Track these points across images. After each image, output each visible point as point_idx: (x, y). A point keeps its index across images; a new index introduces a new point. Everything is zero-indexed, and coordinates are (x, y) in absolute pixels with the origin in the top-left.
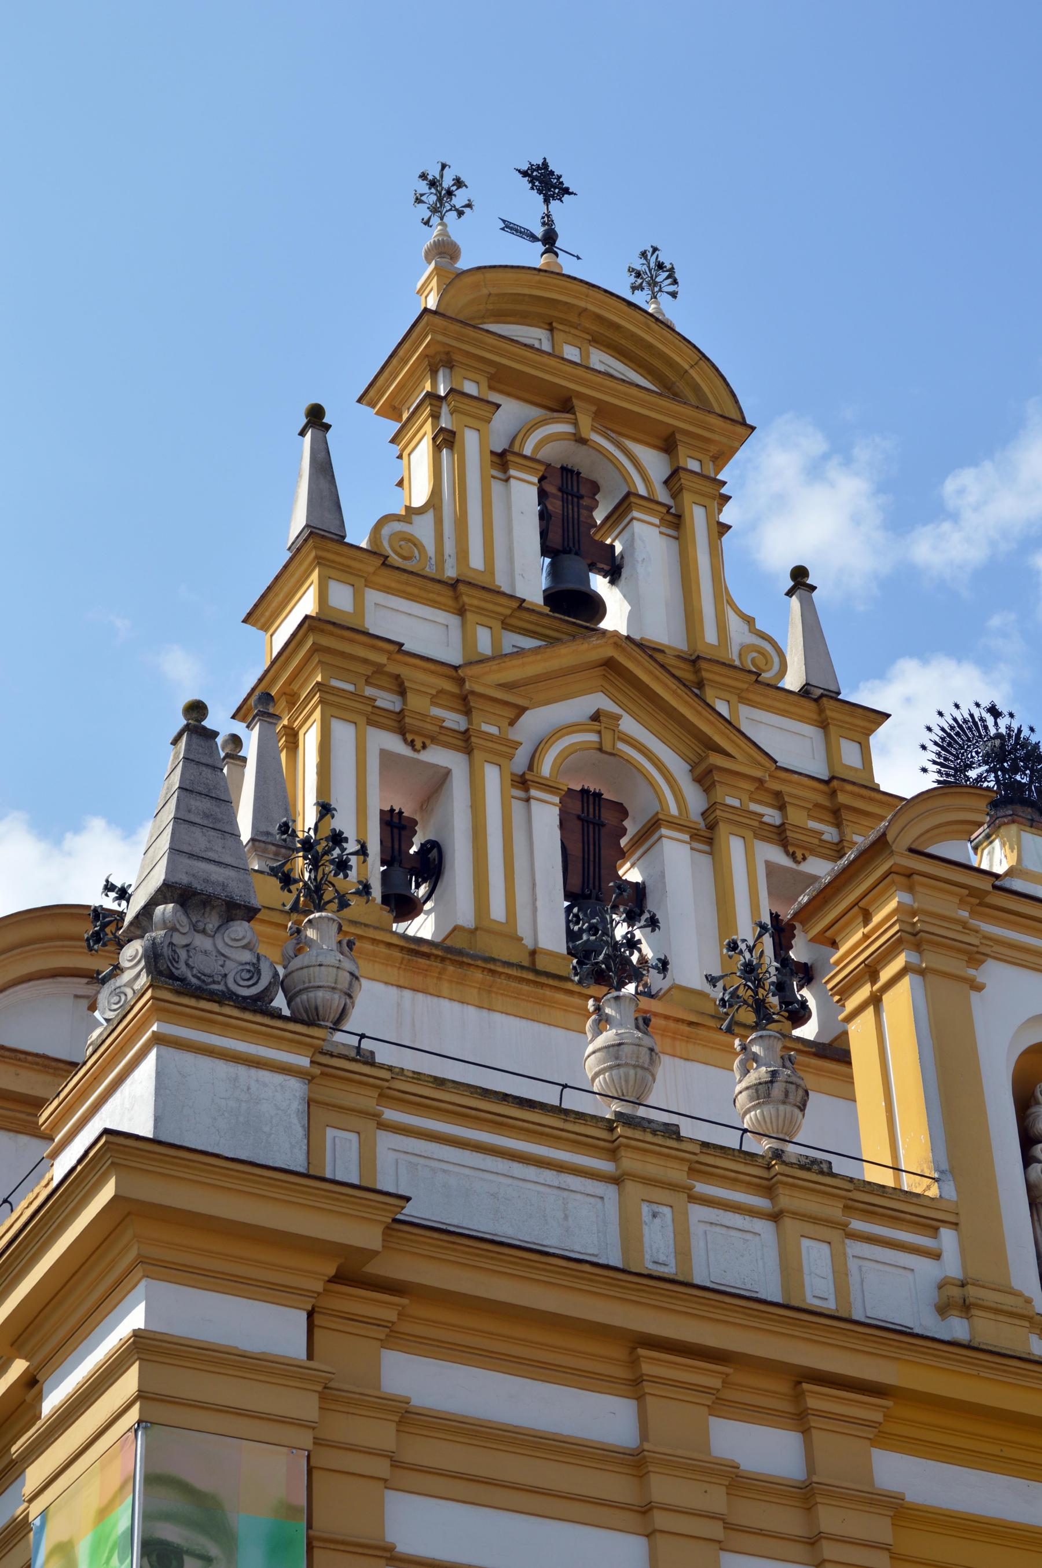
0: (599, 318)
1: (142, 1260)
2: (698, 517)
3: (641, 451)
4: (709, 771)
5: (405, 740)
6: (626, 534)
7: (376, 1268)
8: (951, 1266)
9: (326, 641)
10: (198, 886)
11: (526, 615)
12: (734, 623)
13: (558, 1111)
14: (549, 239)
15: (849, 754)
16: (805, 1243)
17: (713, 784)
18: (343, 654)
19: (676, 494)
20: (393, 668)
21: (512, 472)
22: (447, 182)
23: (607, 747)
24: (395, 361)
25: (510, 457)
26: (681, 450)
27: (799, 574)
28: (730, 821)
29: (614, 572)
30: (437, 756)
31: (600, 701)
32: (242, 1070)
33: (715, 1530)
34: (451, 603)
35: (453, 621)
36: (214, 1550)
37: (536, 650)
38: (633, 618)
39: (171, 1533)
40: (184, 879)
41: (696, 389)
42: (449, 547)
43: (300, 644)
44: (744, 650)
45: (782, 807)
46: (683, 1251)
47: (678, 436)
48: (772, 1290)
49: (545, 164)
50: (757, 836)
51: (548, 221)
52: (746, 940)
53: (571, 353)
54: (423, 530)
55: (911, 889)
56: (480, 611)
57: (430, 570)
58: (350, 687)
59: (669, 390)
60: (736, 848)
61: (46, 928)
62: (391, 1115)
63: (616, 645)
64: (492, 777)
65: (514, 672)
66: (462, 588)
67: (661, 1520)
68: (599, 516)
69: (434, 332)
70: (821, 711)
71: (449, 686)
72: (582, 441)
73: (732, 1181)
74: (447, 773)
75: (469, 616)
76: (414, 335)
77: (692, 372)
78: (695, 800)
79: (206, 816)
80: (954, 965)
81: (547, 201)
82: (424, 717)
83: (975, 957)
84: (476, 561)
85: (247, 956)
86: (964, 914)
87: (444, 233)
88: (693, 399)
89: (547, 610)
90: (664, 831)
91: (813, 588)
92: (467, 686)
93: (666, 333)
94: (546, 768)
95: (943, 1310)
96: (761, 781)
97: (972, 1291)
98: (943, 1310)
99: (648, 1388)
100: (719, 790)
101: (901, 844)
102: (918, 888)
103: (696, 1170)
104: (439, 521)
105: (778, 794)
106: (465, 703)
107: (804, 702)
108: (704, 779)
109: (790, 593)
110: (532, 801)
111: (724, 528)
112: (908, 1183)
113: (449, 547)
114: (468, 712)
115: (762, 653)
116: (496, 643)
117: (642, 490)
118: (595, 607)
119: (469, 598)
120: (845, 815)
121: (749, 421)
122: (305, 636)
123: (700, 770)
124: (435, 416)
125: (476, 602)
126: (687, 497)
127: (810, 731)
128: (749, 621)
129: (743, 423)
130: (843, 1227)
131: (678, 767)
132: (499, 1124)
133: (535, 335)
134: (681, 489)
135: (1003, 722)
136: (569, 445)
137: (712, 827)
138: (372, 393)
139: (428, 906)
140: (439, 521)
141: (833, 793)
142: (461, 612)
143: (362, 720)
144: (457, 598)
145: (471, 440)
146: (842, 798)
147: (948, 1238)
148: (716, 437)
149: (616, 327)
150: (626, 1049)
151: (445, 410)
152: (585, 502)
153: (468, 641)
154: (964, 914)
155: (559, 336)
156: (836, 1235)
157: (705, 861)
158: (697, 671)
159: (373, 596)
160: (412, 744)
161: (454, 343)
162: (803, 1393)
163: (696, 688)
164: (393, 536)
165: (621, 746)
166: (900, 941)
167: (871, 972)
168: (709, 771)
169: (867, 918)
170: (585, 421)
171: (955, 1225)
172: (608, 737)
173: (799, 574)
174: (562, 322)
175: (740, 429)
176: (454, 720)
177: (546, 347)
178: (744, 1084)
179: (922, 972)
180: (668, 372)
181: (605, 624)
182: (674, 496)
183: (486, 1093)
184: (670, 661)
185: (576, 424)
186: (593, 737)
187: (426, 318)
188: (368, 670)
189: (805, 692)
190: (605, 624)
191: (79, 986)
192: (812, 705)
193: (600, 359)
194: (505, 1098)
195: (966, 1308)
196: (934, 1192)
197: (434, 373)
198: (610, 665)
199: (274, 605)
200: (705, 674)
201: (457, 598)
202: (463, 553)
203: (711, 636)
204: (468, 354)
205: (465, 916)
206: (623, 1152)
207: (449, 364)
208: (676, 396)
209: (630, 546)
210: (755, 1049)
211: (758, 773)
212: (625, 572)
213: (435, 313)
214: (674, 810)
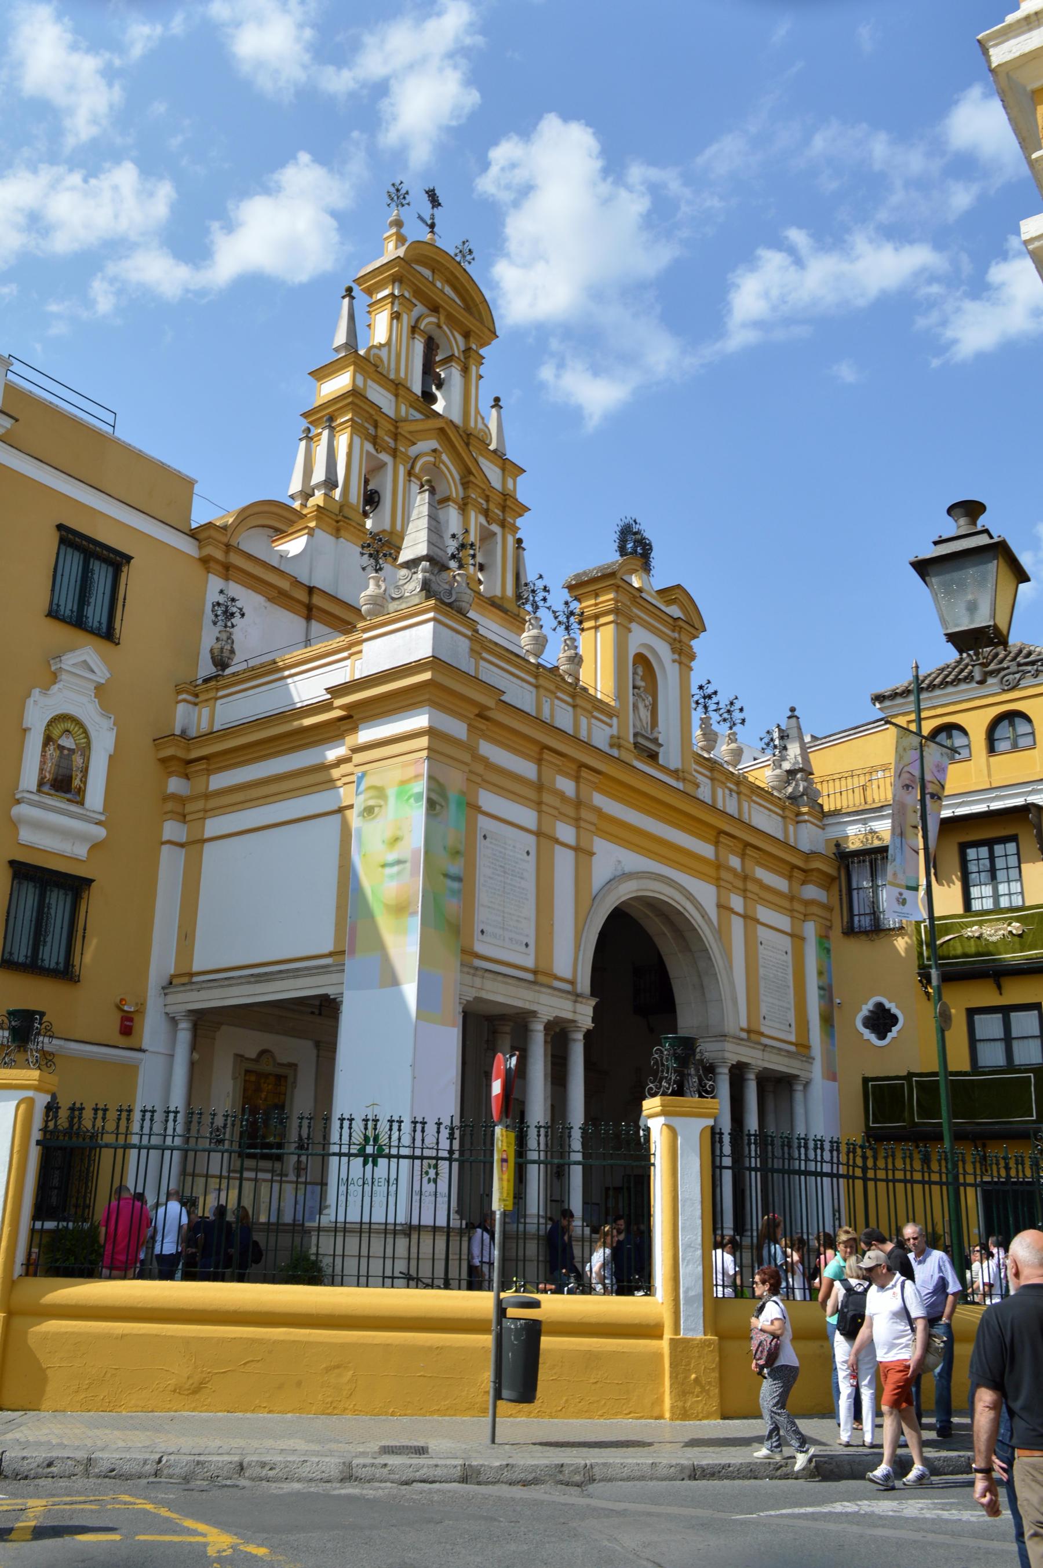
0: (452, 273)
1: (429, 700)
2: (473, 369)
3: (456, 334)
4: (468, 482)
5: (375, 447)
6: (447, 371)
7: (490, 714)
8: (614, 731)
9: (357, 401)
10: (435, 557)
11: (418, 402)
12: (480, 420)
13: (524, 659)
14: (432, 226)
16: (582, 717)
17: (468, 488)
18: (360, 407)
19: (467, 358)
20: (376, 417)
21: (416, 336)
22: (403, 191)
23: (437, 464)
24: (377, 271)
25: (417, 330)
26: (471, 339)
27: (497, 400)
28: (473, 505)
29: (439, 387)
30: (385, 457)
32: (454, 634)
33: (555, 813)
34: (394, 391)
35: (392, 398)
36: (443, 804)
37: (422, 420)
38: (445, 408)
39: (434, 797)
40: (431, 554)
41: (480, 313)
42: (393, 365)
43: (345, 398)
45: (487, 502)
46: (552, 716)
47: (472, 333)
48: (571, 731)
49: (433, 190)
50: (480, 513)
51: (433, 217)
52: (548, 591)
53: (439, 284)
54: (384, 353)
55: (617, 592)
56: (404, 397)
57: (385, 373)
58: (360, 421)
59: (468, 308)
60: (473, 514)
61: (266, 508)
62: (485, 655)
63: (446, 423)
64: (402, 471)
65: (413, 427)
66: (400, 386)
67: (544, 808)
68: (438, 359)
69: (399, 266)
70: (504, 464)
71: (392, 428)
72: (439, 327)
73: (564, 692)
74: (383, 465)
75: (400, 399)
76: (390, 265)
77: (480, 306)
79: (436, 528)
80: (625, 622)
81: (433, 208)
82: (384, 440)
83: (631, 620)
84: (402, 374)
85: (447, 587)
86: (629, 603)
87: (398, 215)
88: (477, 317)
89: (422, 400)
90: (450, 503)
91: (501, 408)
92: (399, 430)
93: (474, 286)
94: (417, 469)
95: (611, 746)
96: (484, 490)
97: (622, 741)
98: (611, 746)
99: (544, 763)
100: (470, 490)
101: (619, 576)
102: (620, 593)
103: (558, 687)
104: (389, 351)
105: (488, 496)
106: (396, 436)
107: (493, 454)
108: (466, 485)
109: (492, 407)
110: (412, 483)
111: (481, 377)
112: (599, 696)
113: (393, 365)
114: (396, 440)
115: (486, 434)
116: (407, 412)
117: (456, 354)
118: (433, 399)
119: (401, 392)
120: (507, 509)
121: (497, 334)
122: (349, 396)
123: (465, 480)
124: (393, 303)
125: (403, 393)
126: (472, 361)
127: (498, 471)
128: (483, 419)
129: (494, 333)
130: (591, 713)
132: (508, 661)
133: (427, 273)
134: (469, 357)
135: (637, 526)
136: (434, 327)
137: (465, 504)
138: (361, 280)
139: (371, 515)
140: (389, 351)
141: (505, 500)
142: (397, 396)
143: (363, 437)
144: (397, 389)
145: (405, 317)
146: (508, 503)
147: (615, 719)
148: (484, 337)
149: (457, 278)
150: (541, 639)
151: (396, 302)
152: (434, 352)
153: (397, 409)
154: (629, 603)
155: (436, 276)
156: (589, 715)
157: (461, 517)
158: (468, 439)
159: (370, 382)
160: (377, 450)
161: (405, 273)
162: (580, 771)
163: (467, 444)
164: (374, 354)
165: (441, 465)
166: (612, 611)
167: (596, 617)
168: (468, 482)
169: (597, 596)
170: (442, 319)
171: (617, 717)
172: (438, 459)
173: (497, 400)
174: (438, 270)
175: (493, 336)
176: (392, 443)
177: (431, 279)
178: (565, 655)
179: (617, 624)
180: (470, 303)
181: (433, 407)
182: (465, 358)
183: (507, 650)
184: (461, 433)
185: (439, 319)
186: (432, 459)
187: (398, 260)
188: (367, 415)
189: (495, 451)
190: (433, 407)
191: (271, 532)
192: (501, 461)
193: (448, 290)
194: (512, 652)
195: (619, 746)
196: (613, 703)
197: (393, 283)
198: (442, 430)
199: (326, 372)
200: (471, 441)
201: (397, 389)
202: (398, 370)
203: (472, 424)
204: (410, 280)
205: (387, 526)
206: (540, 678)
207: (401, 282)
208: (471, 314)
209: (449, 376)
210: (568, 642)
211: (484, 487)
212: (444, 387)
213: (402, 259)
214: (454, 495)
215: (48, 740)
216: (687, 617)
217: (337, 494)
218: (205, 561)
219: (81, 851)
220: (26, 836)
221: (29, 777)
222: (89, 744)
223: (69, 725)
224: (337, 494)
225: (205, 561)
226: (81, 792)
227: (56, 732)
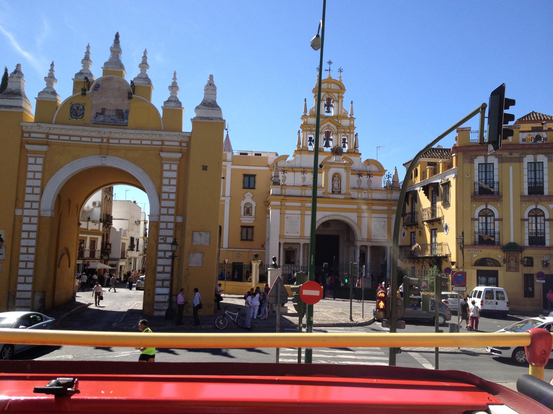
2: (340, 100)
12: (343, 110)
14: (330, 70)
15: (352, 122)
31: (329, 123)
44: (344, 113)
60: (339, 135)
78: (336, 130)
83: (330, 169)
128: (345, 110)
131: (335, 127)
147: (324, 189)
203: (340, 113)
215: (245, 207)
216: (349, 161)
217: (301, 146)
218: (271, 170)
219: (252, 222)
220: (243, 222)
221: (242, 214)
222: (252, 206)
223: (248, 204)
224: (301, 146)
225: (271, 170)
226: (251, 213)
227: (246, 206)
